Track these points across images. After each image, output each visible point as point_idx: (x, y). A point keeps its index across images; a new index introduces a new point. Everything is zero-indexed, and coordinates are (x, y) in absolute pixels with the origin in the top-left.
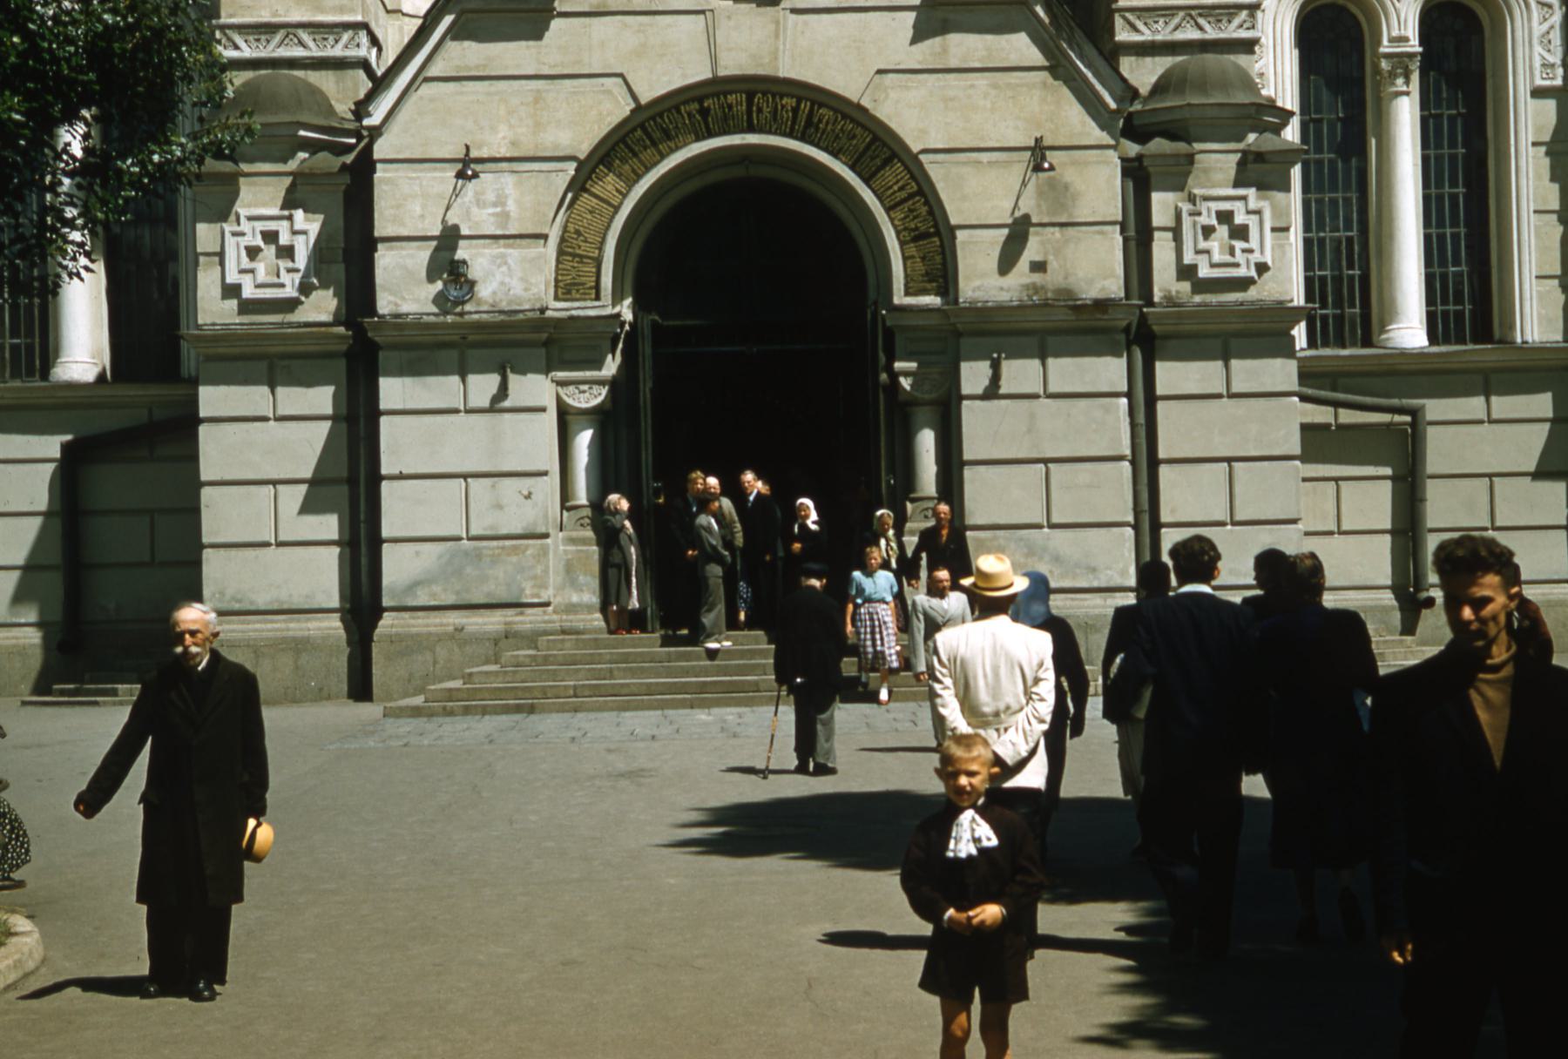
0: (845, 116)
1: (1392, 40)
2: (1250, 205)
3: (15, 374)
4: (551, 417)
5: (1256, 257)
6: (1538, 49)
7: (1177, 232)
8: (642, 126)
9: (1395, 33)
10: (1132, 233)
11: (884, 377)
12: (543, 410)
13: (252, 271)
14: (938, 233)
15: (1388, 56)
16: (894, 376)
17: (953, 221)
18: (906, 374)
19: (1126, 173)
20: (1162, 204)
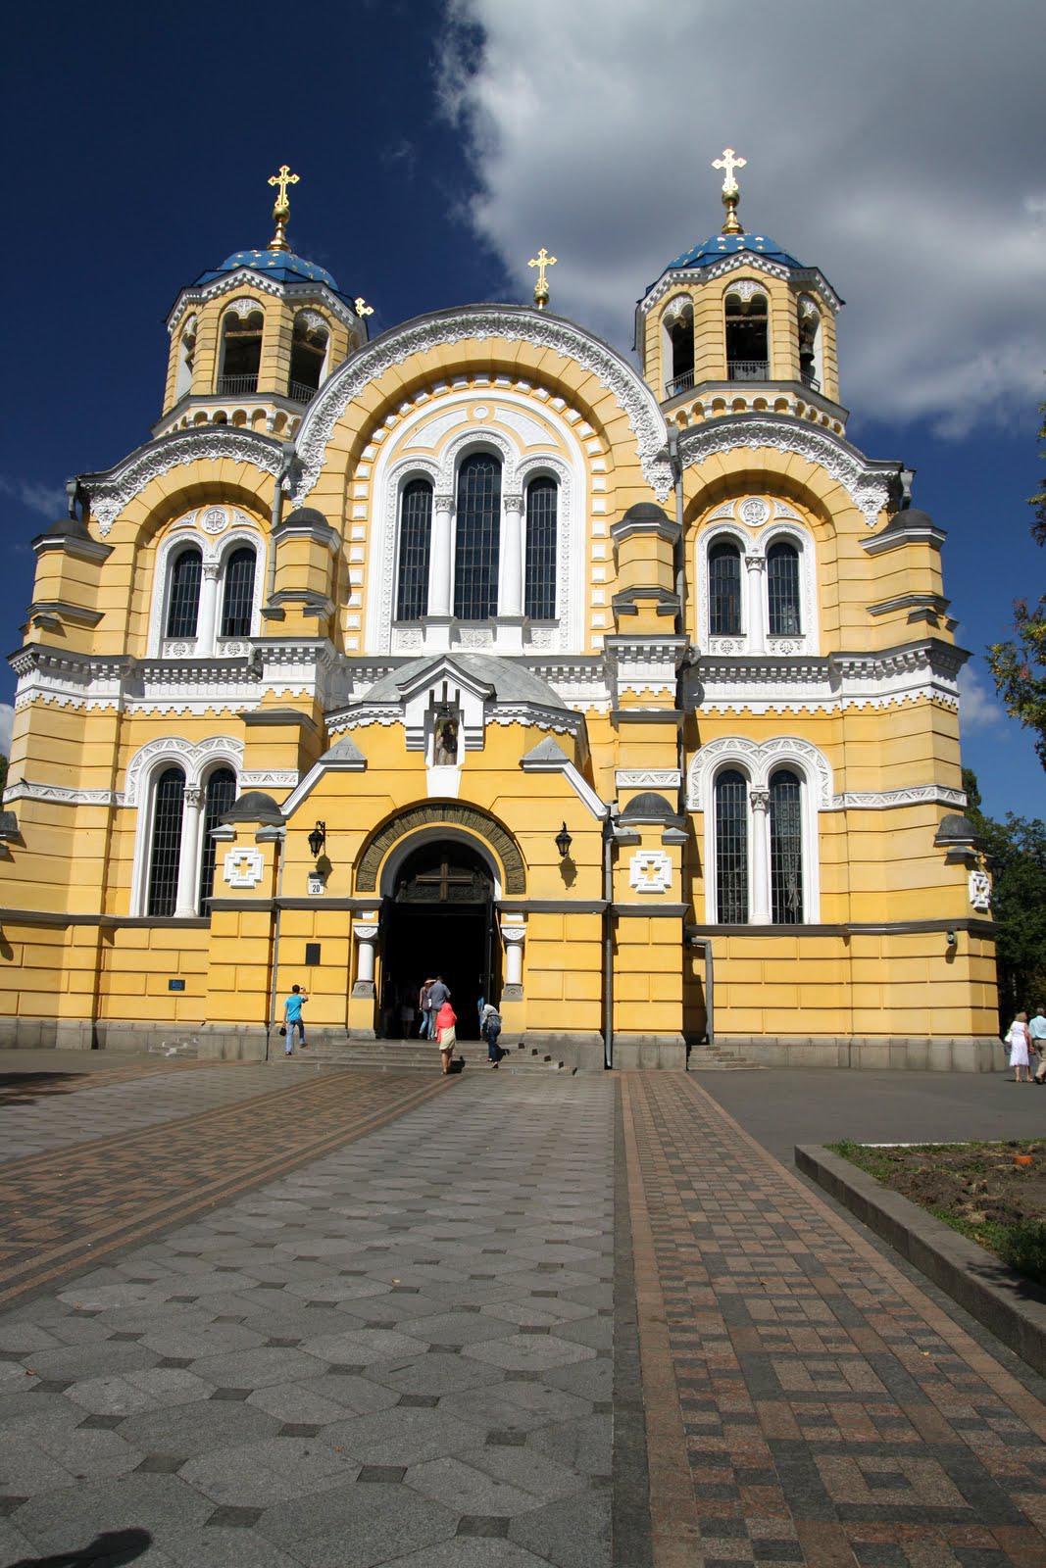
9: (759, 784)
14: (523, 867)
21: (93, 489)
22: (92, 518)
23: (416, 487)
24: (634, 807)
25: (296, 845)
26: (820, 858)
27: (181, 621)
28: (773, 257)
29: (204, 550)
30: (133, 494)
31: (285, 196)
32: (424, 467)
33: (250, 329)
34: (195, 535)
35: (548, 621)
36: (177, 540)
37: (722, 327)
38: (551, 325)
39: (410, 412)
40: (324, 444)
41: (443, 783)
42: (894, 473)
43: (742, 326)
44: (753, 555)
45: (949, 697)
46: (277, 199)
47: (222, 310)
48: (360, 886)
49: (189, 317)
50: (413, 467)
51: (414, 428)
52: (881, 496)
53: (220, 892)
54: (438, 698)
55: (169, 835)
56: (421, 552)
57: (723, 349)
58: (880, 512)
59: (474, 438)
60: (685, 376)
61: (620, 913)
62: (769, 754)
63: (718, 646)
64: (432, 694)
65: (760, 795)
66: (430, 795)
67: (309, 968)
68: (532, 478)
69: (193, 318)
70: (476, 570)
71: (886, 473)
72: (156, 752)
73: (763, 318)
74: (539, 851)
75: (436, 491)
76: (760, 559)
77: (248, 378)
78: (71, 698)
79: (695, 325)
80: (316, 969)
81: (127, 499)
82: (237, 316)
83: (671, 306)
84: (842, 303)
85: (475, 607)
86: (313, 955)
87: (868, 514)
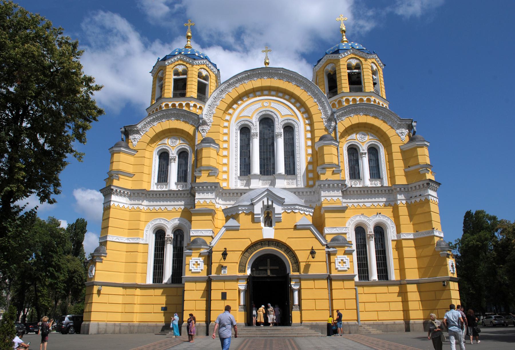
0: (283, 245)
1: (369, 232)
2: (346, 258)
3: (158, 282)
4: (237, 291)
5: (347, 267)
6: (392, 233)
7: (335, 263)
8: (252, 246)
10: (328, 263)
11: (290, 285)
12: (236, 289)
13: (194, 267)
14: (297, 263)
15: (369, 234)
16: (291, 285)
17: (300, 261)
18: (293, 285)
19: (326, 253)
20: (332, 257)
21: (130, 130)
22: (130, 141)
23: (245, 131)
24: (333, 240)
25: (216, 257)
26: (393, 257)
27: (163, 177)
28: (361, 50)
29: (170, 152)
30: (145, 132)
31: (190, 30)
32: (247, 123)
33: (183, 74)
34: (167, 147)
35: (293, 176)
36: (160, 148)
37: (347, 74)
38: (289, 74)
39: (242, 104)
40: (212, 115)
41: (269, 233)
42: (410, 123)
43: (353, 74)
44: (363, 152)
45: (435, 199)
46: (187, 31)
47: (172, 68)
48: (240, 271)
49: (159, 71)
50: (243, 123)
51: (243, 110)
52: (406, 131)
53: (187, 274)
54: (266, 203)
55: (159, 254)
56: (247, 152)
57: (347, 81)
58: (406, 136)
59: (264, 113)
60: (334, 91)
61: (332, 278)
62: (372, 221)
63: (353, 183)
64: (263, 202)
65: (370, 235)
66: (265, 237)
67: (223, 301)
68: (284, 126)
69: (161, 71)
70: (267, 159)
71: (407, 123)
72: (155, 224)
73: (360, 71)
74: (303, 257)
75: (253, 131)
76: (365, 153)
77: (182, 92)
78: (124, 205)
79: (337, 73)
80: (226, 301)
81: (142, 134)
82: (178, 71)
83: (327, 66)
84: (385, 65)
85: (267, 171)
86: (224, 296)
87: (402, 137)
